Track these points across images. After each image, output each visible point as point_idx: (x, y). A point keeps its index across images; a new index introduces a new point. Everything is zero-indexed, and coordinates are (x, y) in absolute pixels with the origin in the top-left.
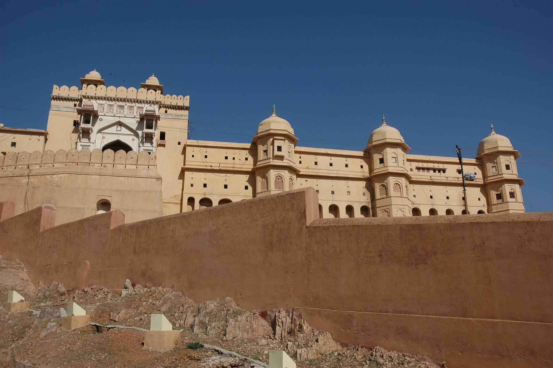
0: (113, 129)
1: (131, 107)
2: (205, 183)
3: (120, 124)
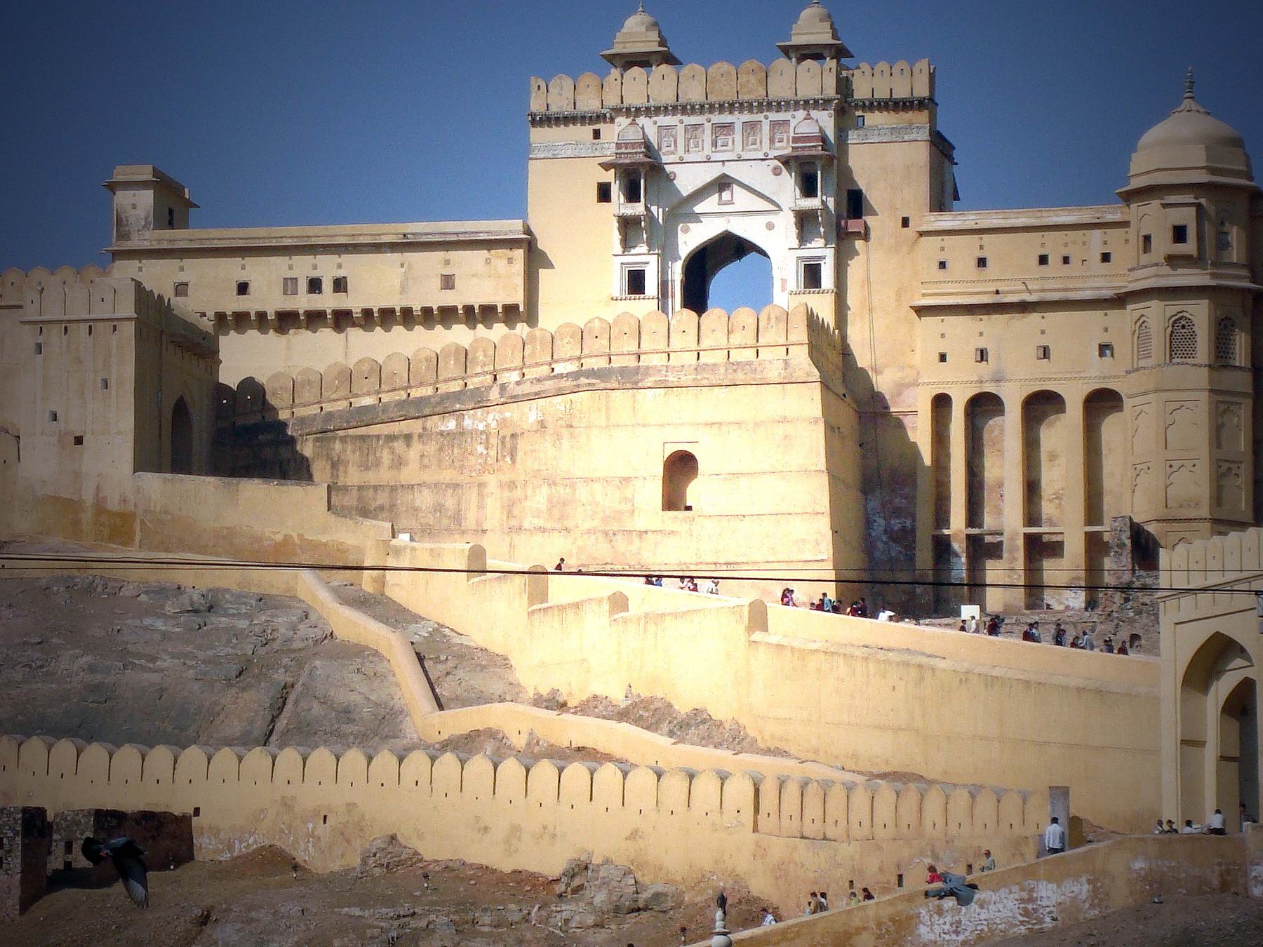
0: (708, 204)
1: (752, 127)
2: (981, 346)
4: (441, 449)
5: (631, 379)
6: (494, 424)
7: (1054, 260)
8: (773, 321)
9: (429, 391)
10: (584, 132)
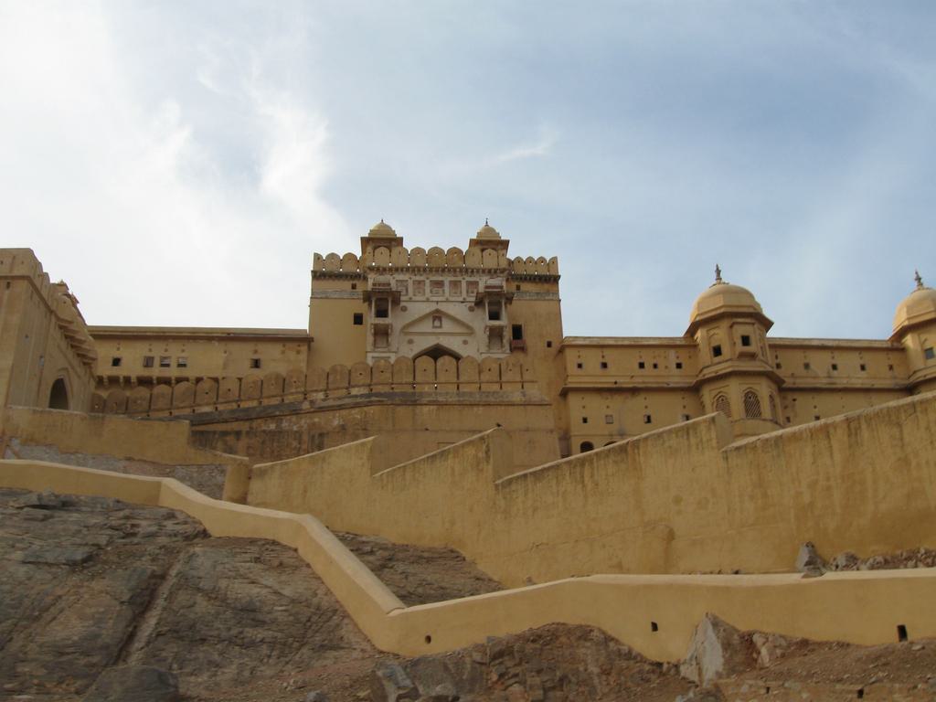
0: (427, 326)
1: (455, 284)
3: (437, 316)
4: (263, 443)
5: (412, 401)
6: (306, 426)
7: (648, 365)
8: (510, 367)
9: (255, 403)
10: (347, 285)
